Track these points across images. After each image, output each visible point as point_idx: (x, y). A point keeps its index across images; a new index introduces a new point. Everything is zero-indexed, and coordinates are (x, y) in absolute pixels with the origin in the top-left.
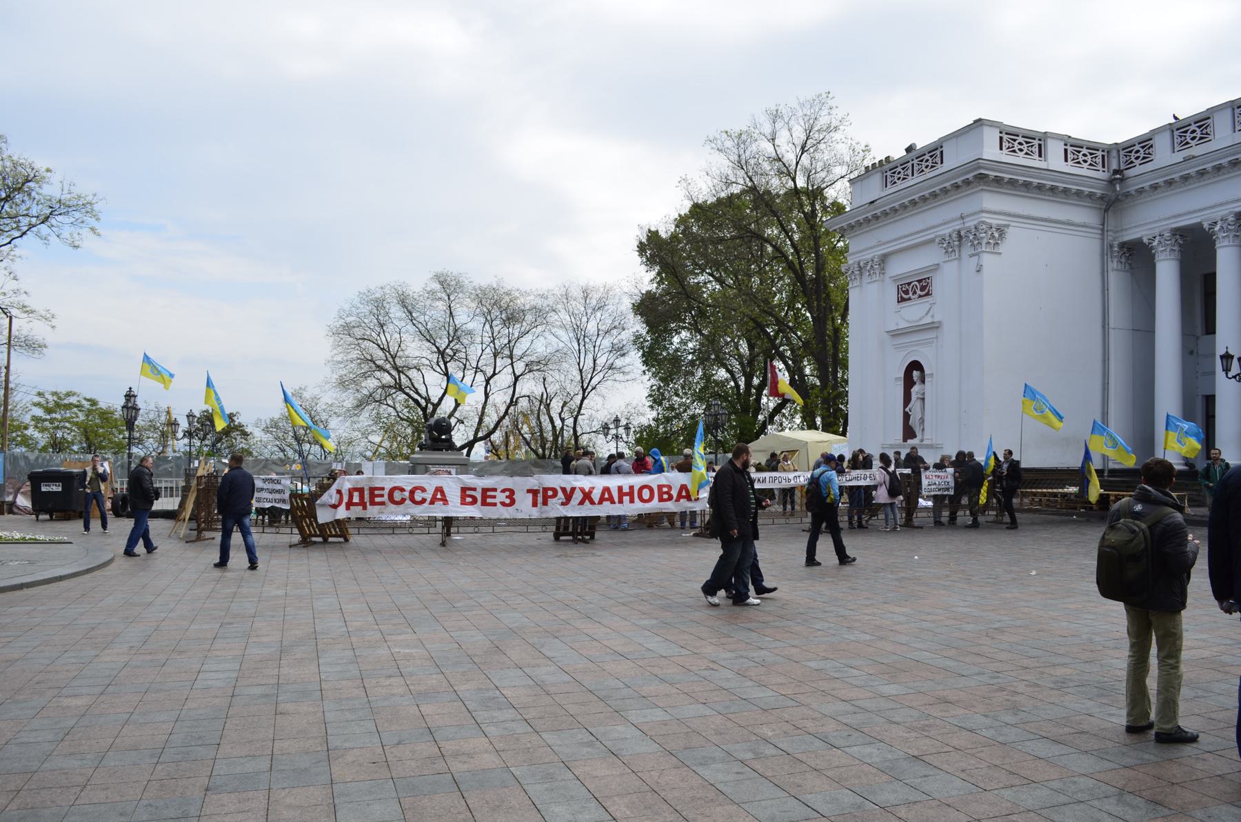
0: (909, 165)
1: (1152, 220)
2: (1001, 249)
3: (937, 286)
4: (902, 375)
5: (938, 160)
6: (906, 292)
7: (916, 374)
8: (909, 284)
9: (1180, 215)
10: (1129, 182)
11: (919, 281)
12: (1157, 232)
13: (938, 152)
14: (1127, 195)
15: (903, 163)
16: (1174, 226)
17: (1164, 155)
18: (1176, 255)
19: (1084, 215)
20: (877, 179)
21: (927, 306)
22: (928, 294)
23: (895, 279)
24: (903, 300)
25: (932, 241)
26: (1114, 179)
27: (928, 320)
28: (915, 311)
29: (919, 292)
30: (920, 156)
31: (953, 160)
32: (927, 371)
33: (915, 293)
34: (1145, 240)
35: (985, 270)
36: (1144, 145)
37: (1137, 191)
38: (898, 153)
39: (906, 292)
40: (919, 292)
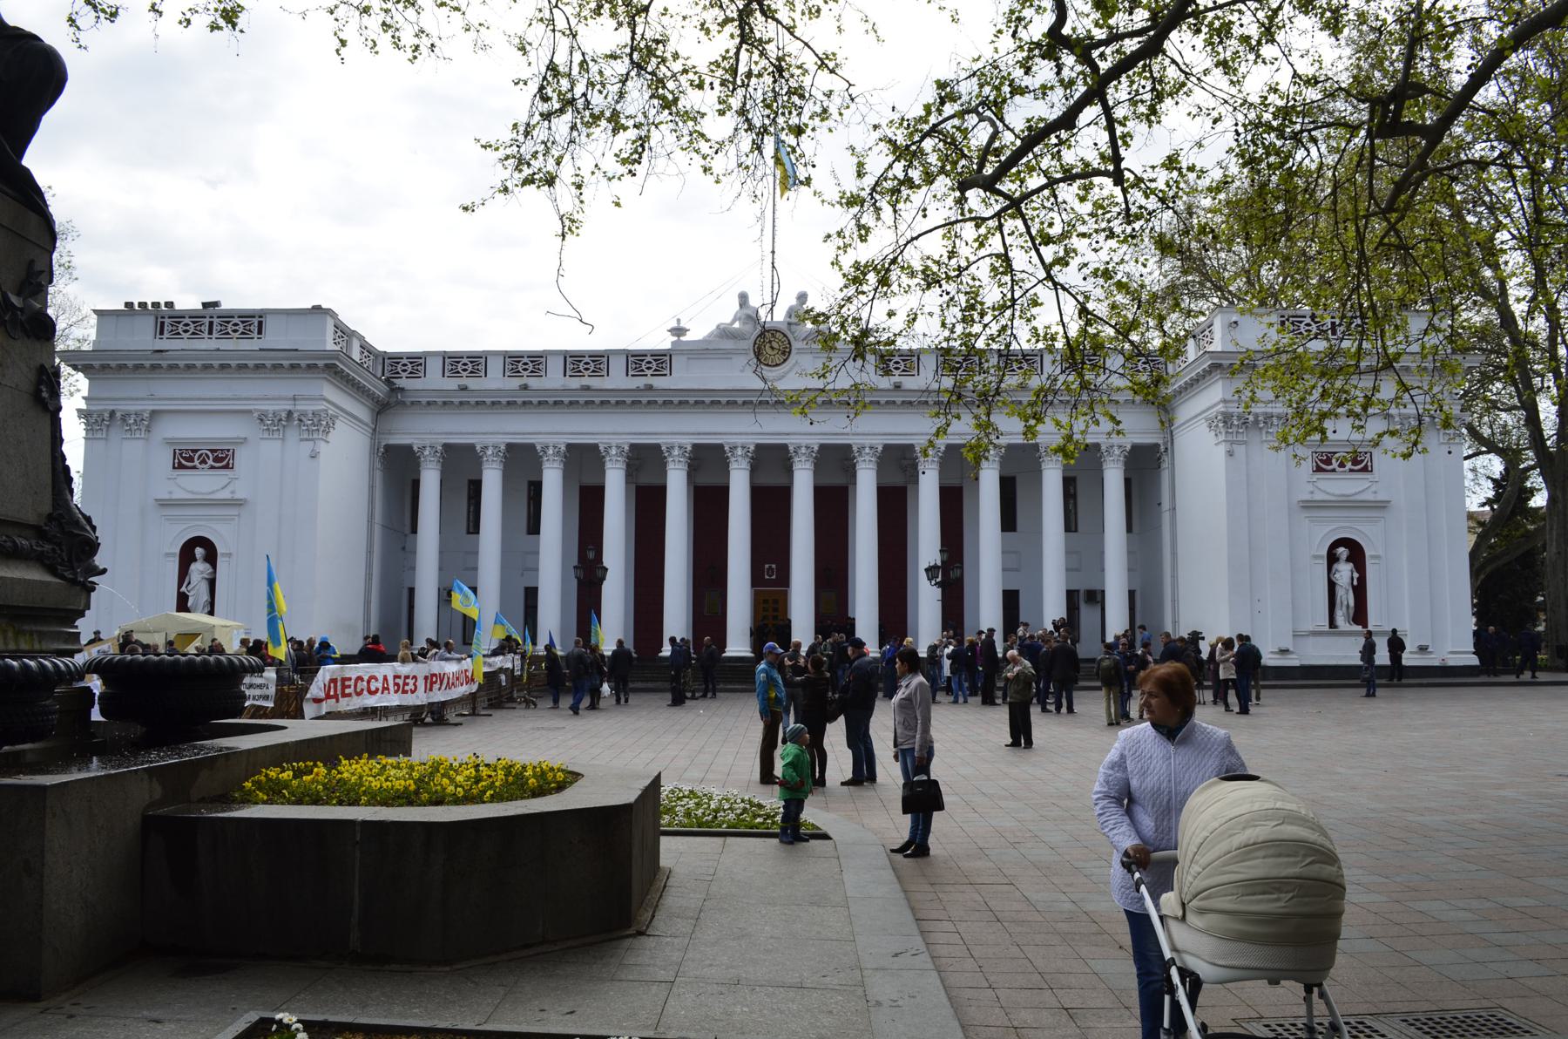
0: (207, 321)
1: (424, 432)
2: (330, 437)
3: (242, 458)
4: (177, 550)
5: (255, 328)
6: (191, 459)
7: (199, 551)
8: (195, 451)
11: (212, 451)
12: (427, 443)
13: (256, 321)
14: (404, 403)
15: (195, 316)
17: (435, 380)
19: (363, 413)
20: (149, 324)
21: (226, 481)
22: (226, 467)
23: (169, 442)
24: (181, 466)
25: (250, 412)
26: (389, 383)
27: (225, 495)
28: (203, 482)
29: (210, 462)
30: (227, 316)
31: (274, 337)
32: (219, 551)
33: (204, 462)
35: (322, 457)
36: (415, 363)
38: (188, 302)
39: (191, 459)
40: (210, 462)
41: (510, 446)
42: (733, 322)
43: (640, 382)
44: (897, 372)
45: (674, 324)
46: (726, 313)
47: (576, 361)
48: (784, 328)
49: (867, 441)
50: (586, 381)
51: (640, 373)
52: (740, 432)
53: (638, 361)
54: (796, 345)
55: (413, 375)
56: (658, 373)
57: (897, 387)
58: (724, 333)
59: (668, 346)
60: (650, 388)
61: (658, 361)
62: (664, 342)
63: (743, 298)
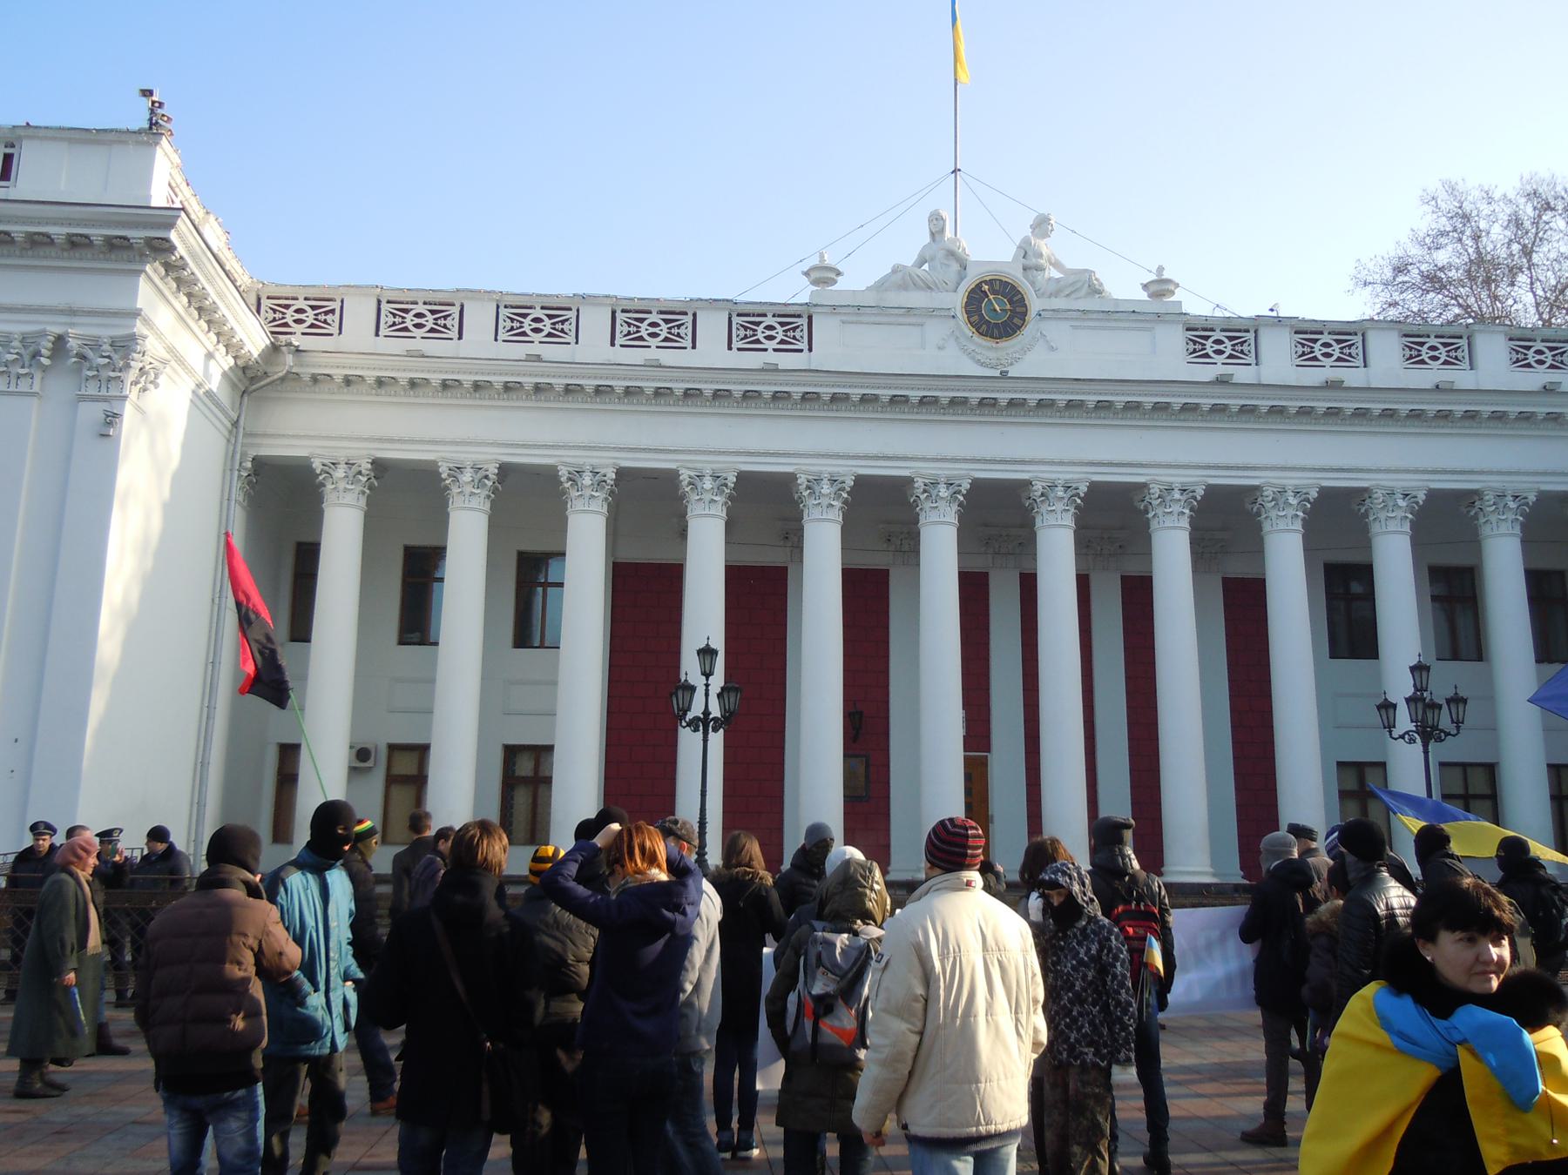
1: (331, 435)
9: (391, 440)
10: (307, 358)
12: (341, 456)
16: (380, 455)
18: (363, 502)
34: (317, 465)
37: (315, 379)
41: (505, 470)
42: (921, 262)
43: (753, 360)
44: (1220, 359)
45: (815, 261)
46: (905, 246)
47: (635, 320)
48: (1017, 276)
49: (1177, 478)
50: (653, 354)
51: (754, 346)
52: (939, 456)
53: (748, 323)
54: (1035, 304)
55: (315, 329)
56: (785, 347)
57: (1222, 381)
58: (900, 279)
59: (804, 298)
60: (775, 369)
61: (793, 324)
62: (796, 291)
63: (936, 221)
